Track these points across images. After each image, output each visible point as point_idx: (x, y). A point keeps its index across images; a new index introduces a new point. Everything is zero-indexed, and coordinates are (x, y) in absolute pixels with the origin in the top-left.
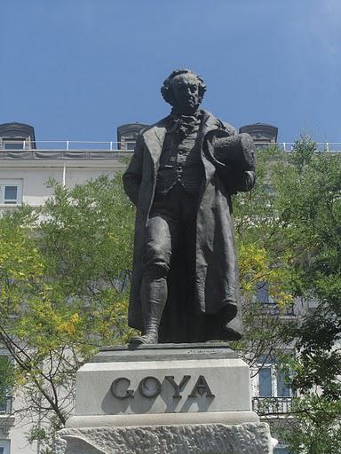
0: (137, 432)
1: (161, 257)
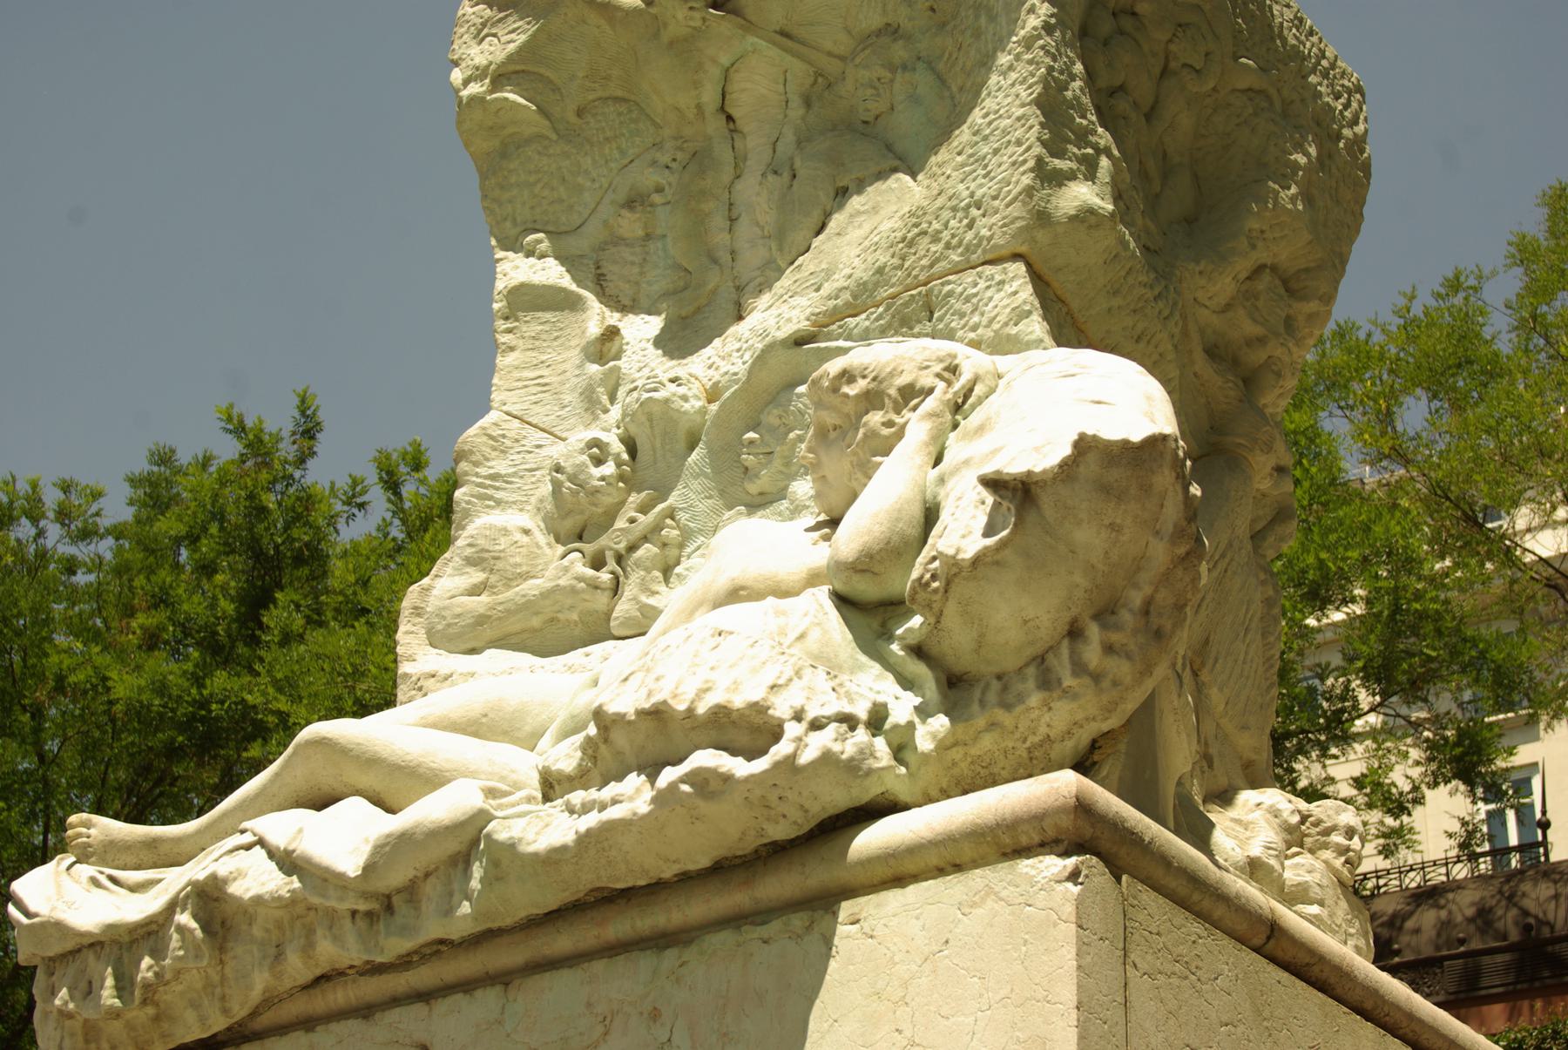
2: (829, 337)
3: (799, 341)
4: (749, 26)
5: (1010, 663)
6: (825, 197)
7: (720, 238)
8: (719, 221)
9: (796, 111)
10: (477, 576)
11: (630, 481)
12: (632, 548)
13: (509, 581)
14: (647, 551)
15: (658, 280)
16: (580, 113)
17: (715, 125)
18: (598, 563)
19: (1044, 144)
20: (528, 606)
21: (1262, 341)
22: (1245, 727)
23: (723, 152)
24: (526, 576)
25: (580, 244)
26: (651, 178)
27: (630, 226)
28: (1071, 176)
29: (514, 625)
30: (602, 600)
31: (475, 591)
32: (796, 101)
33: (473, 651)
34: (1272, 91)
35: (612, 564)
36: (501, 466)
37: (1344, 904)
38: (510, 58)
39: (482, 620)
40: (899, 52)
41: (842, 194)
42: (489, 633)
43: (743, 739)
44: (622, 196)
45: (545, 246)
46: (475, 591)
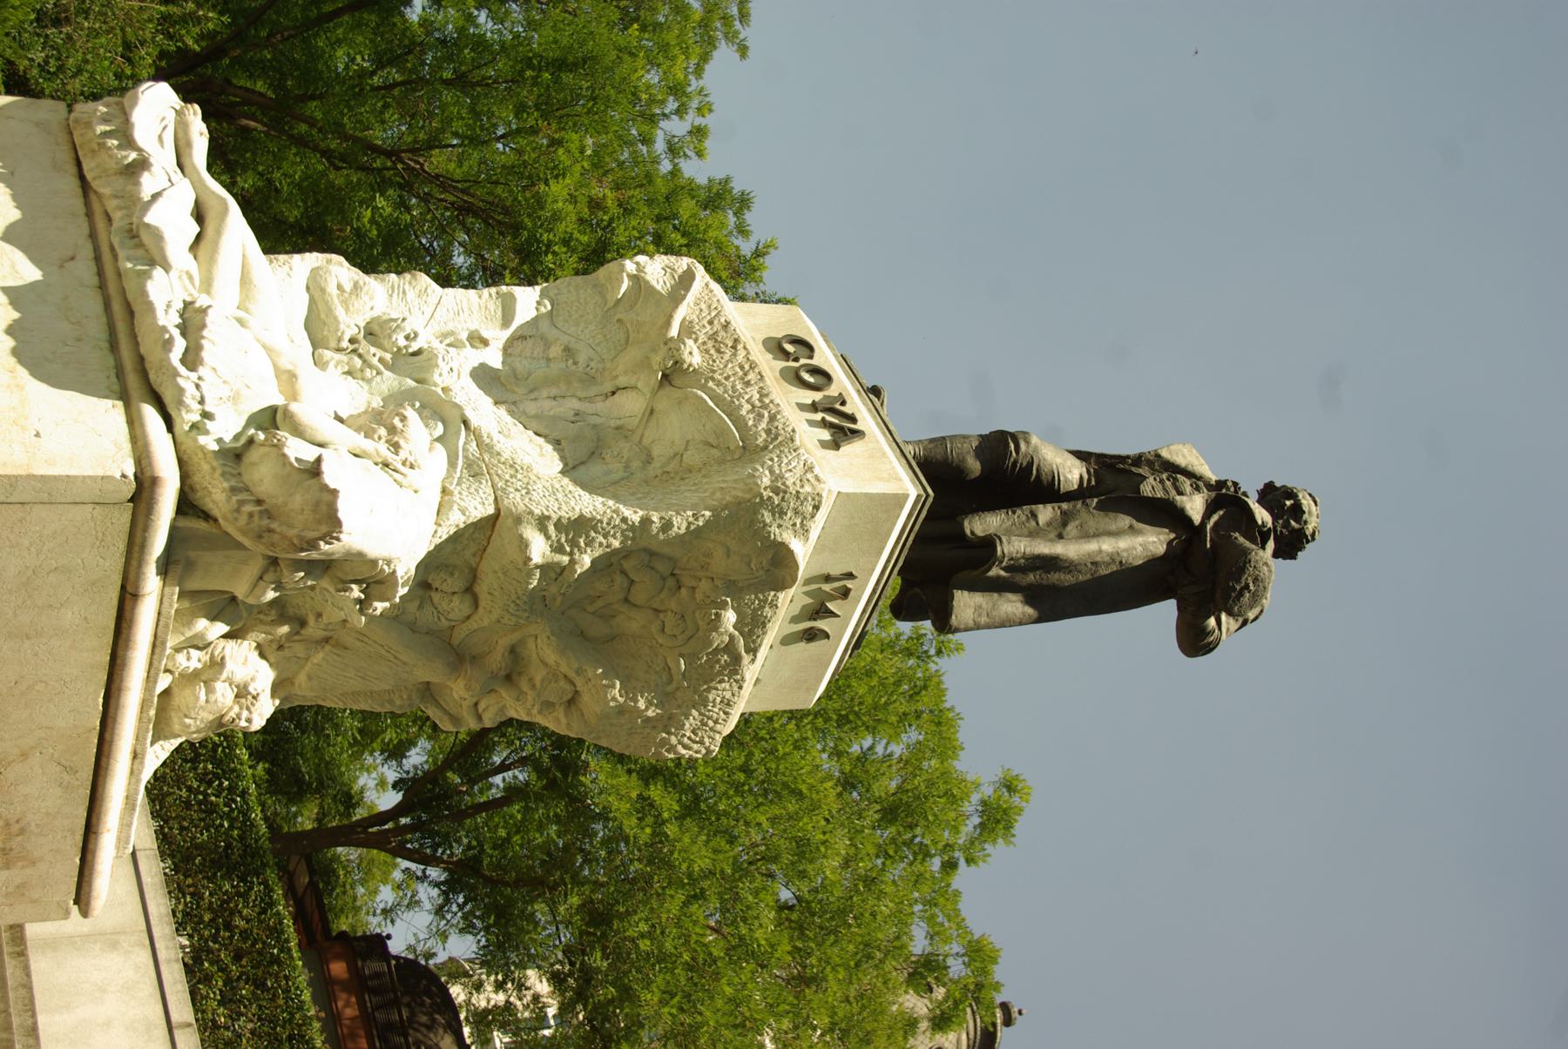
0: (736, 341)
1: (1023, 446)
2: (467, 436)
3: (465, 422)
4: (655, 393)
5: (246, 478)
6: (555, 435)
7: (545, 393)
8: (554, 391)
9: (613, 423)
10: (348, 287)
11: (398, 353)
12: (360, 356)
13: (346, 304)
14: (358, 362)
15: (521, 366)
16: (619, 321)
17: (608, 387)
18: (352, 341)
19: (559, 519)
20: (330, 311)
21: (533, 687)
22: (310, 678)
23: (593, 391)
24: (347, 310)
25: (545, 326)
26: (582, 359)
27: (555, 351)
28: (548, 537)
29: (321, 306)
30: (333, 344)
31: (339, 287)
32: (618, 422)
33: (308, 288)
34: (674, 685)
35: (351, 347)
36: (411, 294)
37: (211, 717)
38: (647, 282)
39: (323, 290)
40: (636, 464)
41: (557, 444)
42: (317, 295)
43: (190, 358)
44: (572, 345)
45: (543, 310)
46: (339, 287)
